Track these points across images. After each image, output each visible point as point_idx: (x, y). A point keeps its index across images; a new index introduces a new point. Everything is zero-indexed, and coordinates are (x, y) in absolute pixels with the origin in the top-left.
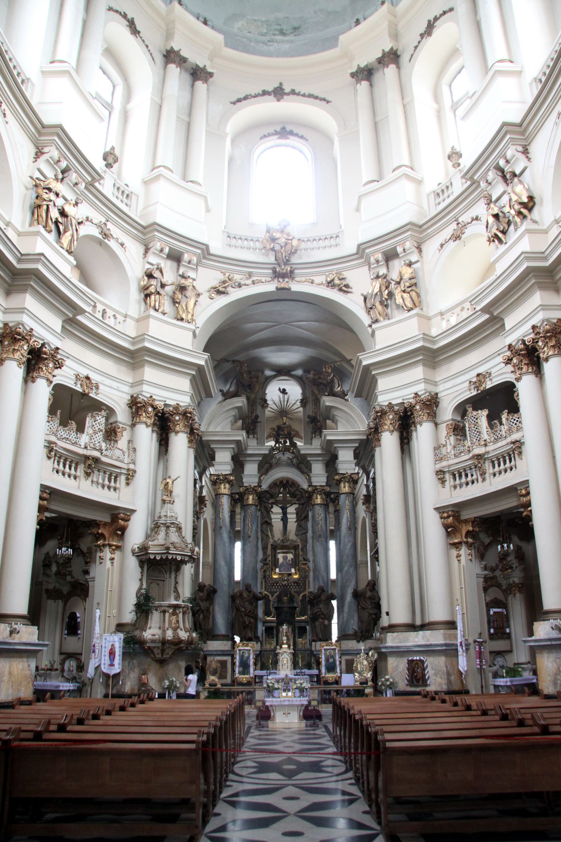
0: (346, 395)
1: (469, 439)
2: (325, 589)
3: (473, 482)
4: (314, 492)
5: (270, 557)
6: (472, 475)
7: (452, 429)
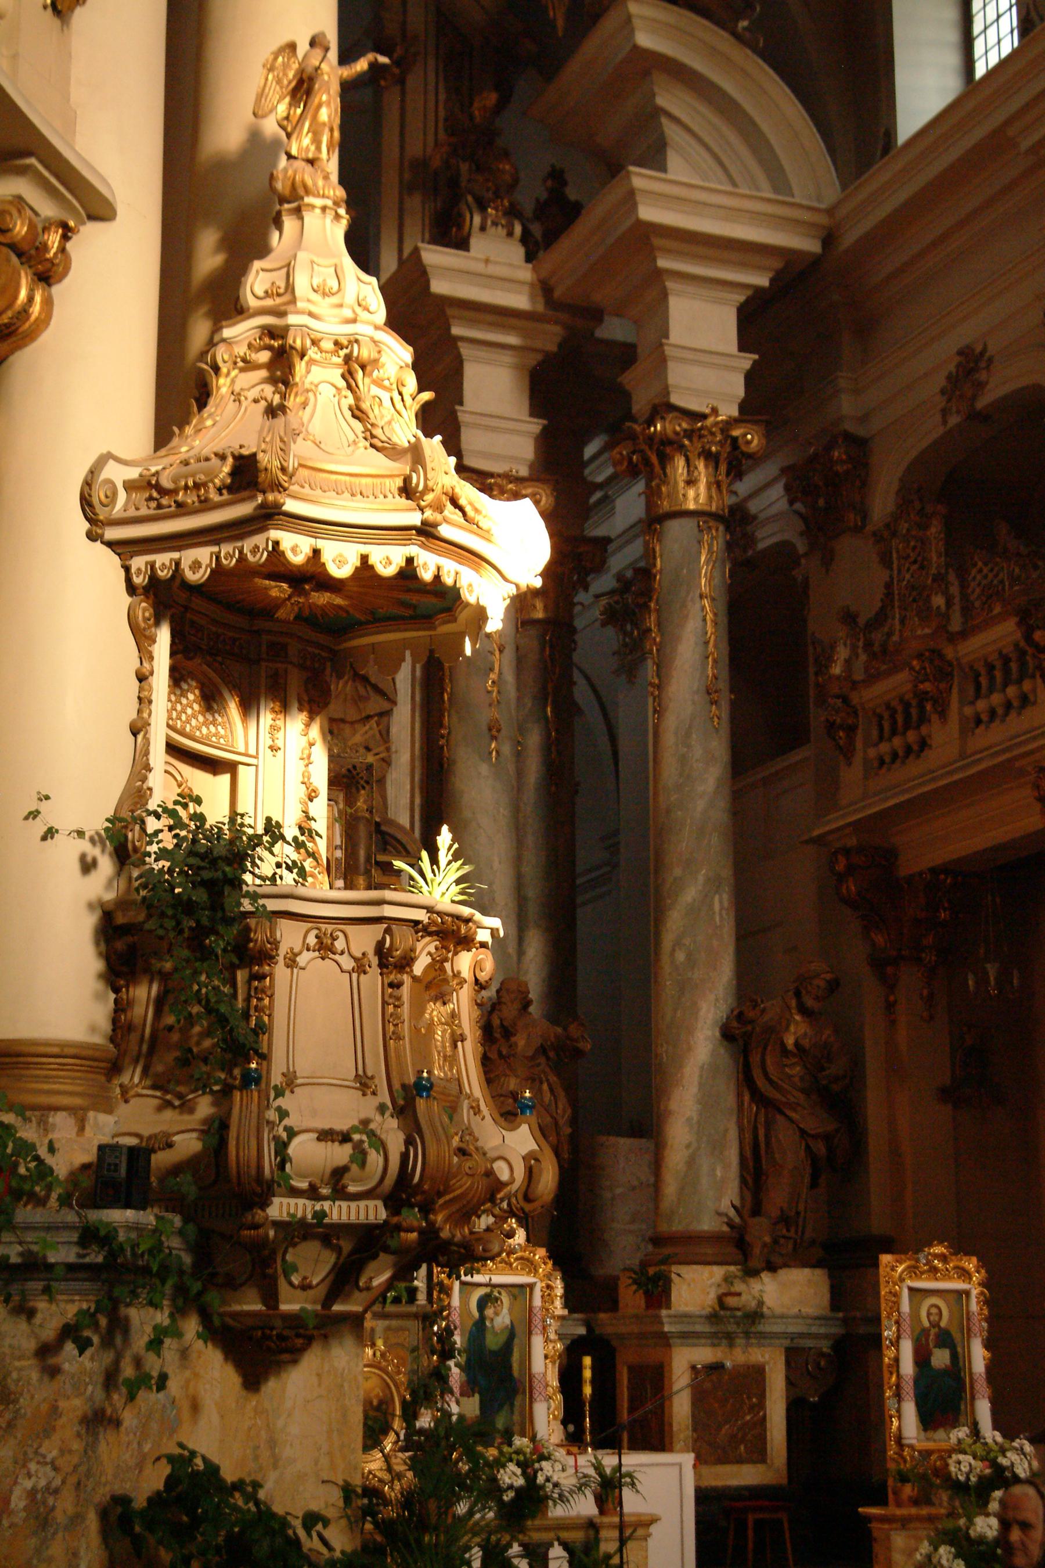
0: (739, 16)
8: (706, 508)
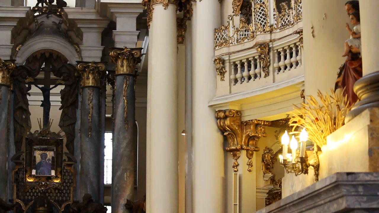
1: (254, 22)
2: (93, 198)
3: (256, 76)
4: (84, 70)
5: (24, 154)
6: (256, 67)
7: (239, 7)
8: (126, 73)
